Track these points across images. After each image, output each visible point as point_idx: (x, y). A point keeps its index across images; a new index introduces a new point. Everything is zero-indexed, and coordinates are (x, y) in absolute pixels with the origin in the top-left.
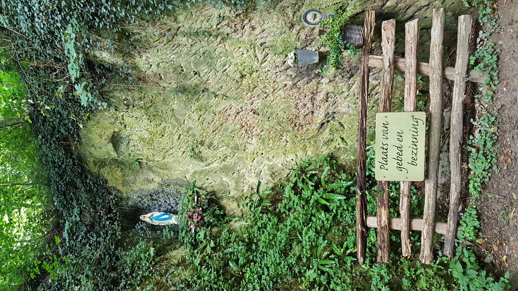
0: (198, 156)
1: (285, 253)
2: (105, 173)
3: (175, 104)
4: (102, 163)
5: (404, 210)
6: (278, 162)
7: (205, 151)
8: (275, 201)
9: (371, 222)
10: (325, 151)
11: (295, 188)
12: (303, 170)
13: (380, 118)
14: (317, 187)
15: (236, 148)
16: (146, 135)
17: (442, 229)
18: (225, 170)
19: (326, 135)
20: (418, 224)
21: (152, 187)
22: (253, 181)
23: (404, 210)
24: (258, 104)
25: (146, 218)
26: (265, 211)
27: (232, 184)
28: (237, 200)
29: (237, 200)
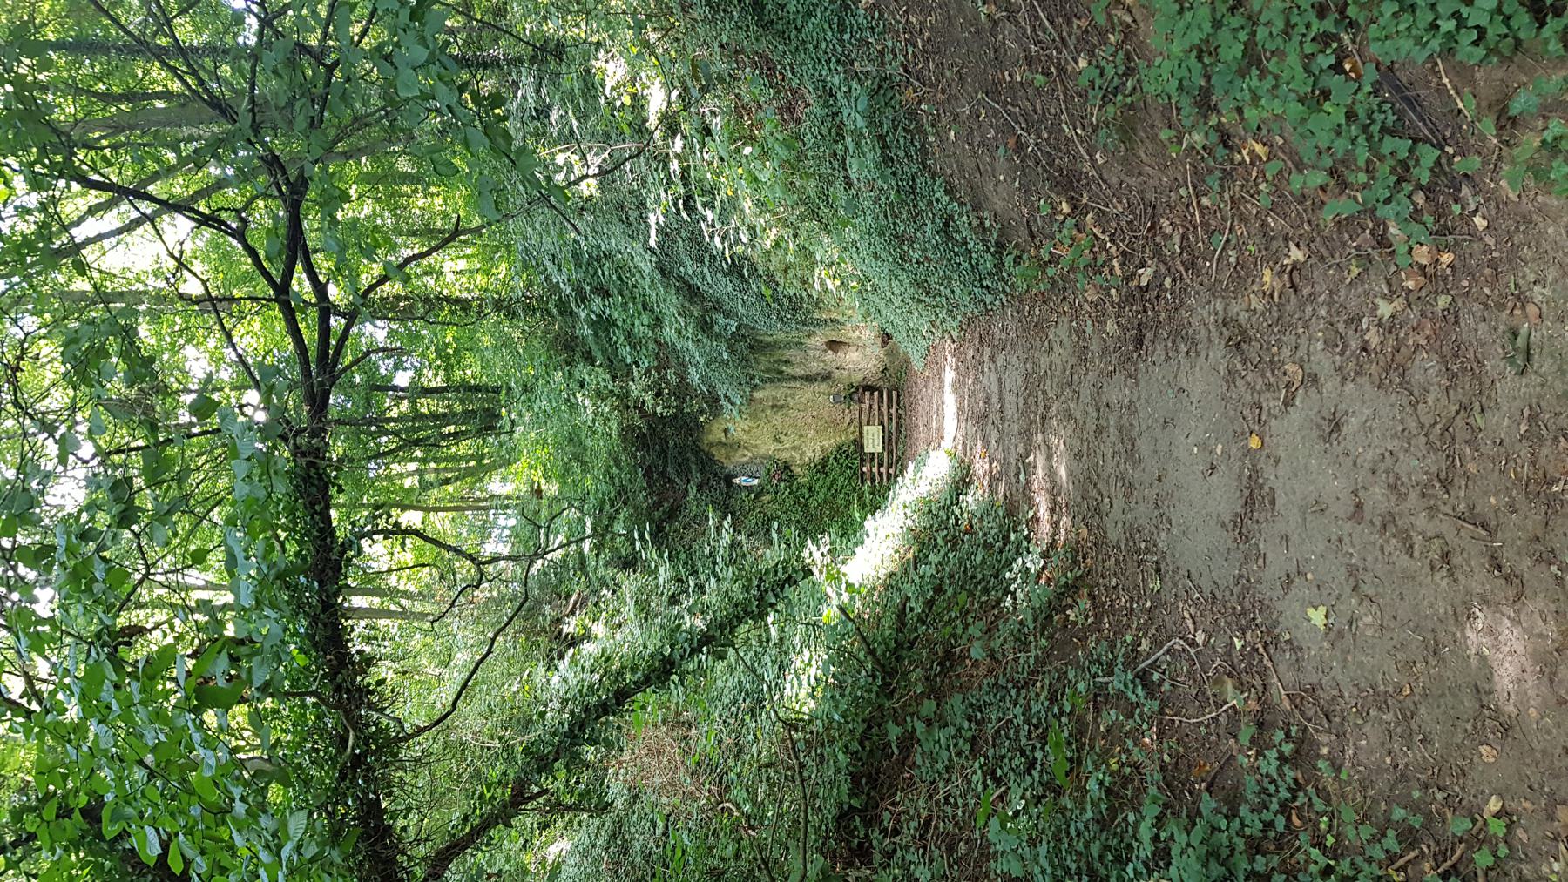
0: (778, 440)
1: (829, 489)
2: (714, 451)
3: (768, 412)
4: (711, 445)
5: (885, 464)
6: (826, 443)
7: (783, 437)
8: (823, 467)
9: (864, 469)
10: (852, 437)
11: (835, 458)
12: (840, 448)
13: (865, 428)
14: (847, 457)
15: (801, 436)
16: (747, 428)
17: (891, 471)
18: (794, 448)
19: (852, 429)
20: (882, 470)
21: (745, 459)
22: (810, 454)
23: (885, 464)
24: (815, 414)
25: (736, 481)
26: (818, 471)
27: (798, 457)
28: (801, 466)
29: (801, 466)
